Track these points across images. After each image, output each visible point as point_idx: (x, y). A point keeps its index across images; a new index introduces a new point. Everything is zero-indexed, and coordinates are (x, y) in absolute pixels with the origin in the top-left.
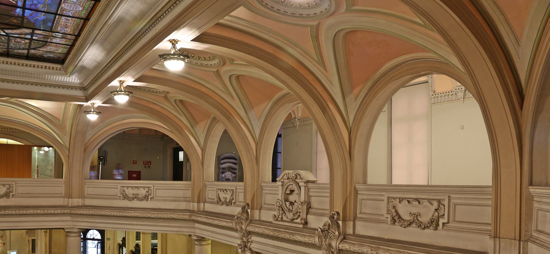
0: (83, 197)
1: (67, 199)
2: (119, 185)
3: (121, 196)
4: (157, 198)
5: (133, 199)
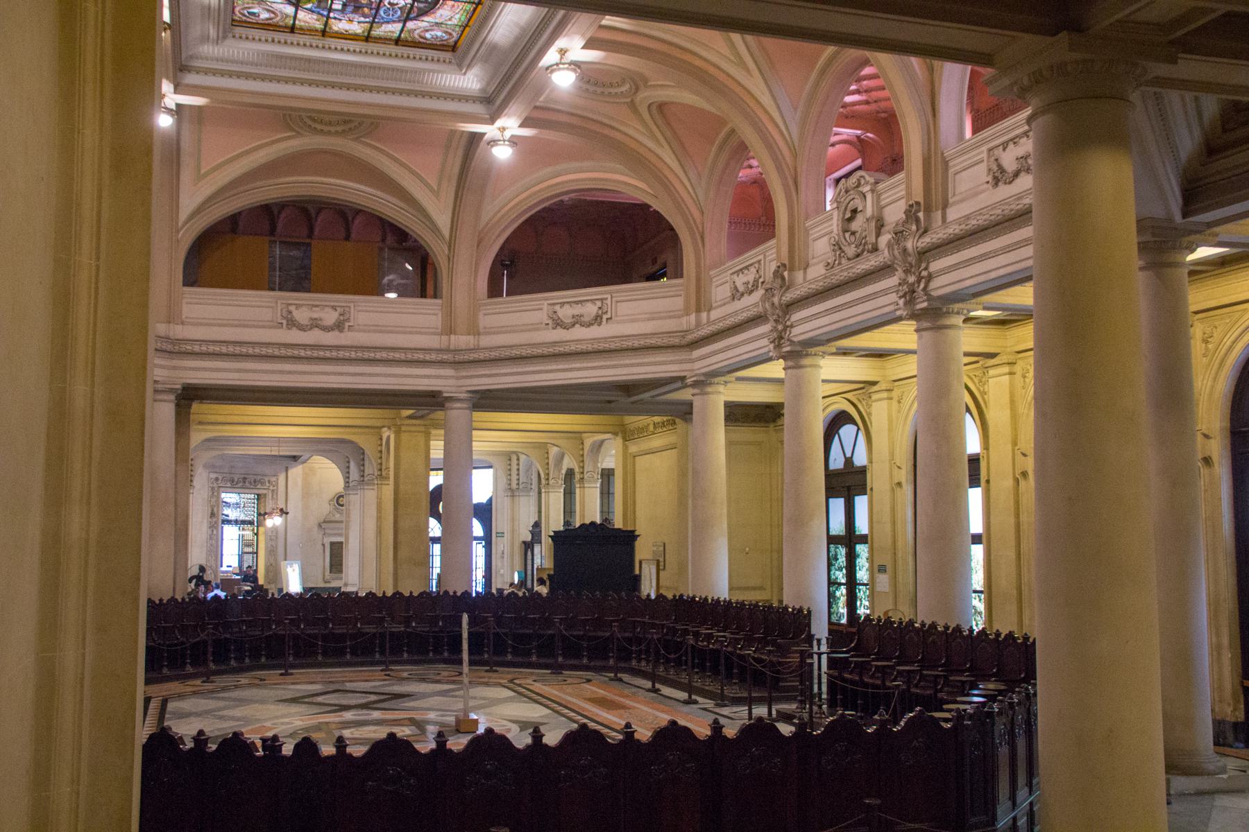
0: (474, 330)
1: (447, 337)
2: (546, 303)
3: (550, 322)
4: (618, 318)
5: (573, 325)
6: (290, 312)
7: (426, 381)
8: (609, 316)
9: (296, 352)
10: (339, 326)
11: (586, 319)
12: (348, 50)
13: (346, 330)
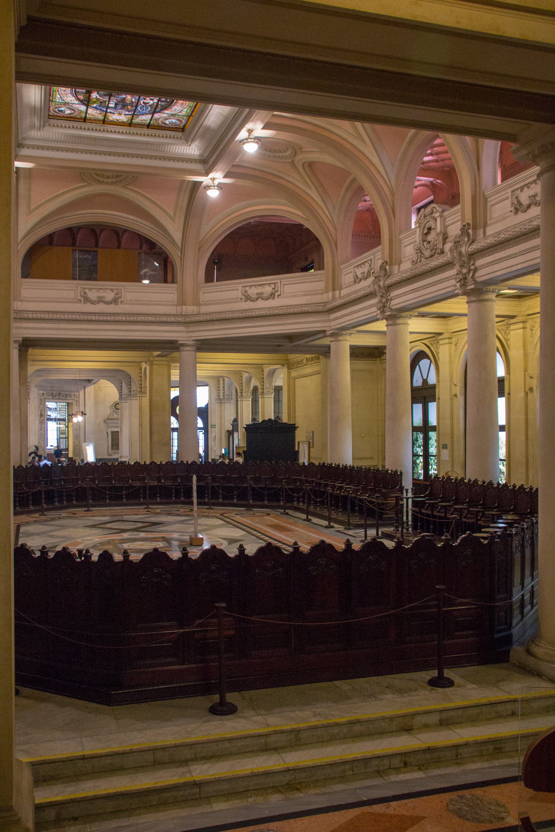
0: (197, 303)
2: (240, 286)
3: (243, 297)
5: (257, 299)
6: (85, 293)
7: (167, 334)
8: (279, 293)
9: (90, 317)
10: (115, 301)
11: (265, 295)
12: (119, 132)
13: (120, 303)
